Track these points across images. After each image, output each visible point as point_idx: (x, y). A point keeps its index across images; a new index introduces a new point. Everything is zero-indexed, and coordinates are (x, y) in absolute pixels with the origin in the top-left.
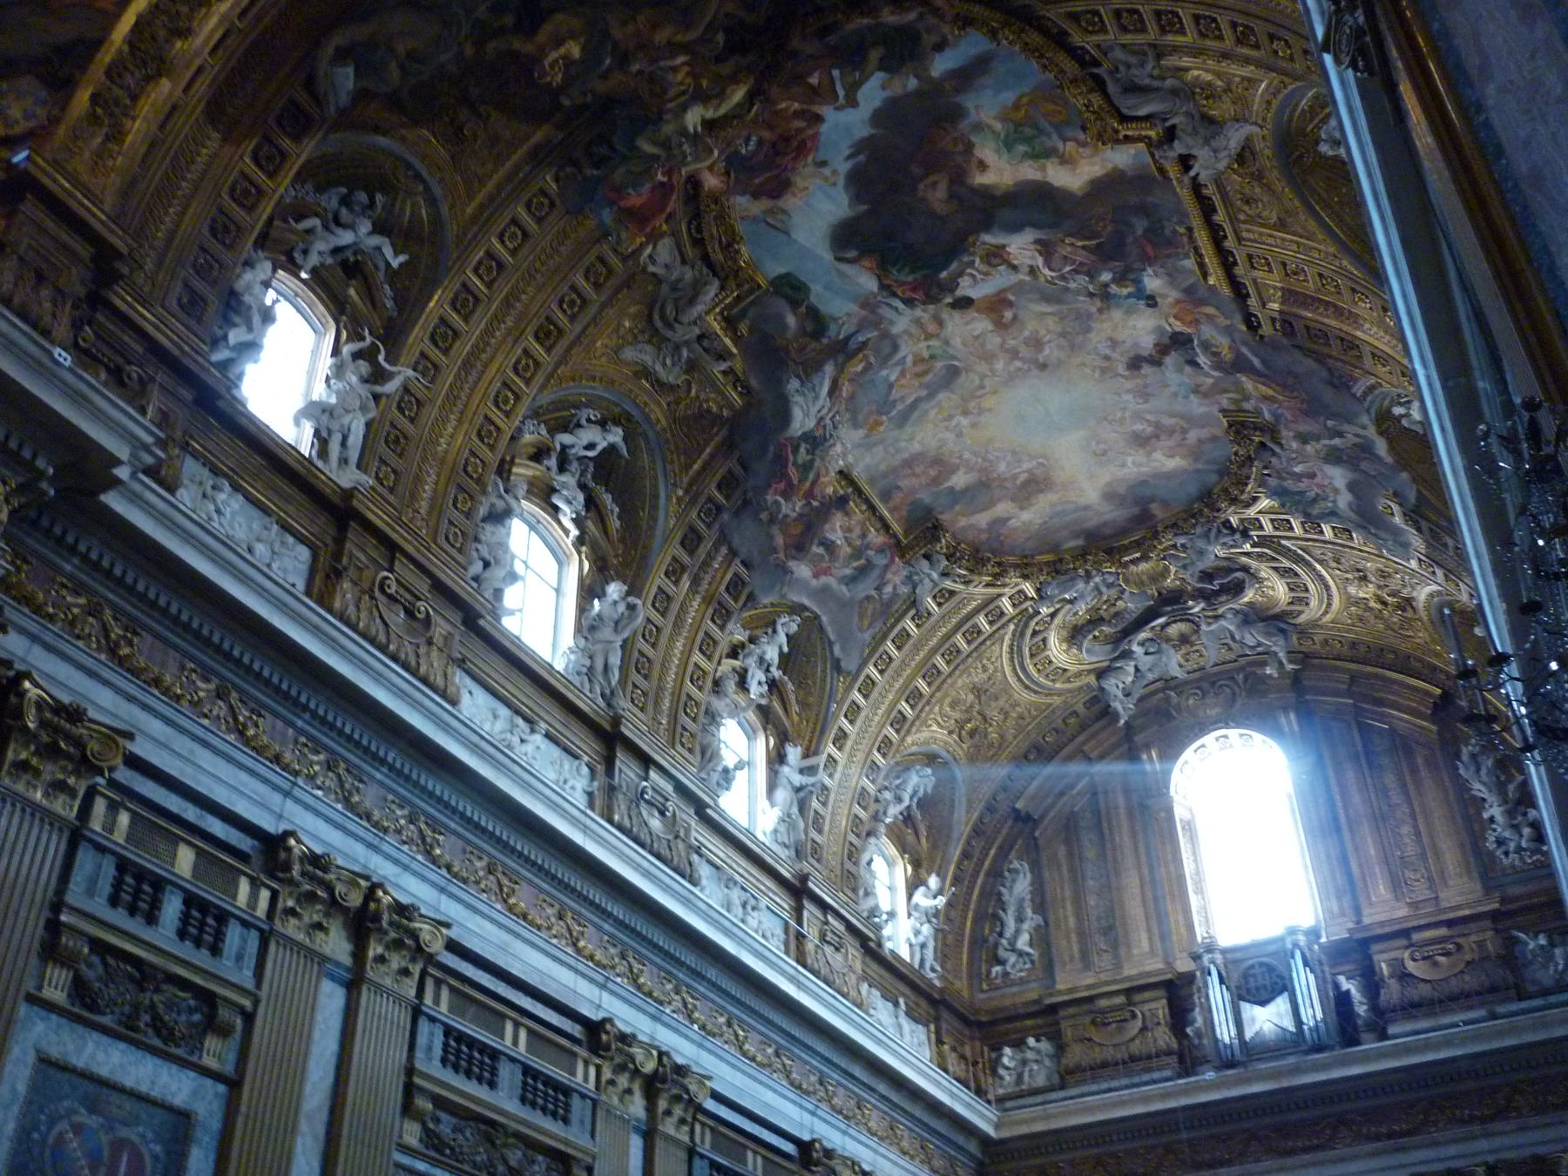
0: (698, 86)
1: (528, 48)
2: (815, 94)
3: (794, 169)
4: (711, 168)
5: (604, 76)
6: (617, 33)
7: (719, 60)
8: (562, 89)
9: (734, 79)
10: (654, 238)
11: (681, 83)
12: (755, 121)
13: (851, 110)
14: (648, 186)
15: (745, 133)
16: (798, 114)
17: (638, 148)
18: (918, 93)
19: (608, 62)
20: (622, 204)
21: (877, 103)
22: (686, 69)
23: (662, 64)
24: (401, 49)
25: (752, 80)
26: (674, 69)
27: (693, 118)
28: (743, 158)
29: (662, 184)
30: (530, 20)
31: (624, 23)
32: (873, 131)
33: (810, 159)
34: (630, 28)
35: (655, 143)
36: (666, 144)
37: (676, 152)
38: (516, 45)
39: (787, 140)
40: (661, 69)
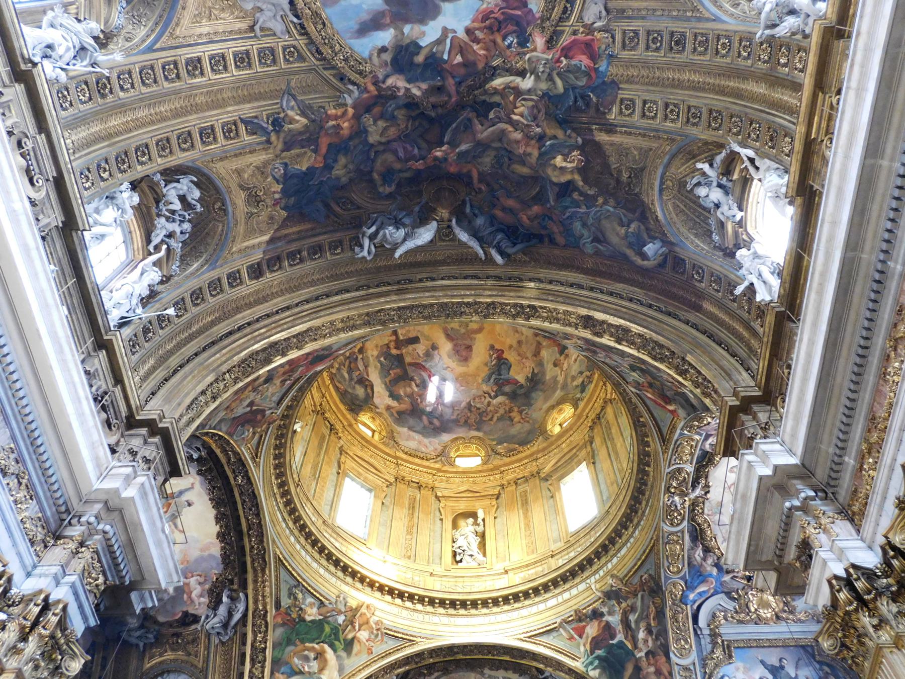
0: (515, 99)
1: (577, 177)
2: (462, 49)
3: (496, 5)
4: (535, 50)
5: (555, 137)
6: (536, 153)
7: (498, 105)
8: (578, 148)
9: (496, 91)
10: (590, 29)
11: (523, 105)
12: (500, 55)
13: (449, 27)
14: (573, 62)
15: (508, 52)
16: (476, 41)
17: (565, 89)
18: (407, 21)
19: (548, 143)
20: (592, 65)
21: (432, 23)
22: (515, 111)
23: (525, 122)
24: (623, 231)
25: (487, 86)
26: (522, 115)
27: (527, 83)
28: (518, 37)
29: (566, 57)
30: (567, 188)
31: (530, 154)
32: (442, 4)
33: (485, 6)
34: (529, 150)
35: (554, 83)
36: (550, 78)
37: (548, 70)
38: (581, 183)
39: (490, 28)
40: (527, 120)
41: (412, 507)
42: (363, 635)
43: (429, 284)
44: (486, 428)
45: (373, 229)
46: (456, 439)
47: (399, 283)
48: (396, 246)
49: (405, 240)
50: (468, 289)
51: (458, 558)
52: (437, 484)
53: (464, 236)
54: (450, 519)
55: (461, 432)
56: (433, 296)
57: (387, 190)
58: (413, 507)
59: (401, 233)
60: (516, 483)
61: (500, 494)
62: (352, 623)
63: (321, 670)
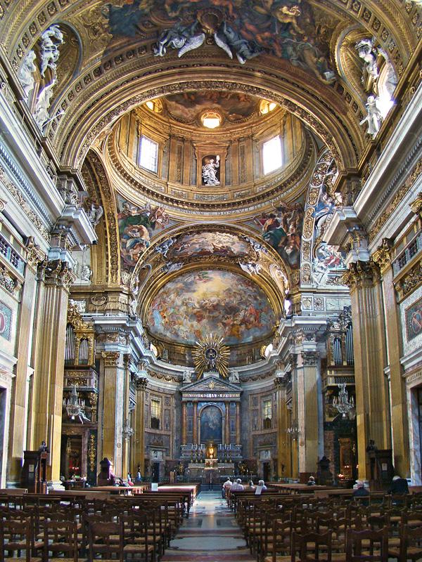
41: (180, 153)
42: (160, 220)
43: (198, 68)
44: (223, 102)
45: (166, 41)
46: (205, 109)
47: (180, 67)
48: (179, 49)
49: (185, 45)
50: (221, 74)
51: (205, 181)
52: (194, 138)
53: (220, 43)
54: (201, 159)
55: (208, 105)
56: (200, 77)
57: (173, 15)
58: (181, 153)
59: (183, 41)
60: (238, 140)
61: (229, 146)
62: (154, 216)
63: (141, 236)
